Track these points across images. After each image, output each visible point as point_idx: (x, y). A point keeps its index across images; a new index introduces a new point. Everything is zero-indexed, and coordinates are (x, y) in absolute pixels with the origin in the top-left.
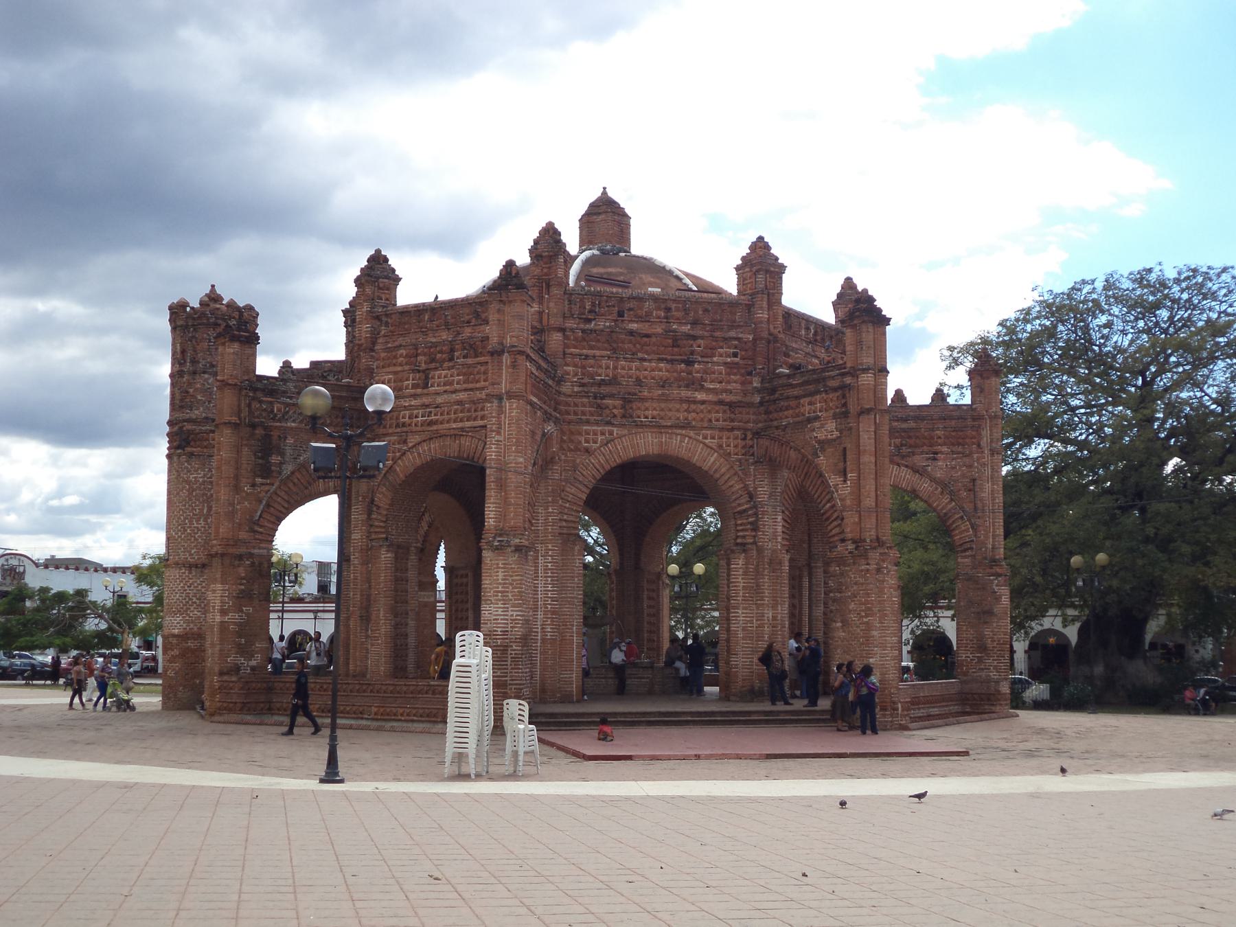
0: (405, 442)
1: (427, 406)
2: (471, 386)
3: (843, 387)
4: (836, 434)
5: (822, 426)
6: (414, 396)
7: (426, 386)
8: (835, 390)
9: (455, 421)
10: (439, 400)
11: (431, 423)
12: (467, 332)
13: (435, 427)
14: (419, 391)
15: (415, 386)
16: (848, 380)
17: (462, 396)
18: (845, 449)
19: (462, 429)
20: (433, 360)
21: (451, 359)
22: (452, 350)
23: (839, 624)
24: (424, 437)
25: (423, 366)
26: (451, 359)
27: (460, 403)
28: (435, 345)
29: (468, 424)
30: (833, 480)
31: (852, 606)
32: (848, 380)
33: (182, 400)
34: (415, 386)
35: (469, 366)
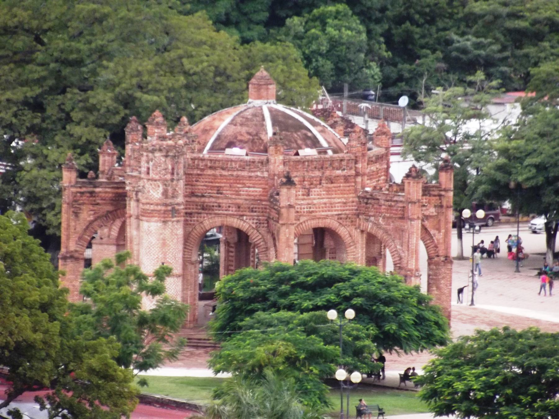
0: (299, 220)
1: (309, 204)
2: (330, 196)
3: (440, 196)
4: (435, 214)
5: (427, 210)
6: (303, 199)
7: (309, 195)
8: (435, 196)
9: (323, 211)
10: (315, 202)
11: (312, 212)
12: (328, 173)
13: (313, 214)
14: (305, 197)
15: (303, 195)
16: (443, 193)
17: (325, 200)
18: (440, 220)
19: (327, 216)
20: (312, 184)
21: (320, 184)
22: (321, 180)
23: (434, 288)
24: (308, 218)
25: (307, 186)
26: (320, 184)
27: (325, 204)
28: (313, 177)
29: (329, 213)
30: (432, 232)
31: (442, 282)
32: (443, 193)
33: (173, 194)
34: (303, 195)
35: (329, 188)
